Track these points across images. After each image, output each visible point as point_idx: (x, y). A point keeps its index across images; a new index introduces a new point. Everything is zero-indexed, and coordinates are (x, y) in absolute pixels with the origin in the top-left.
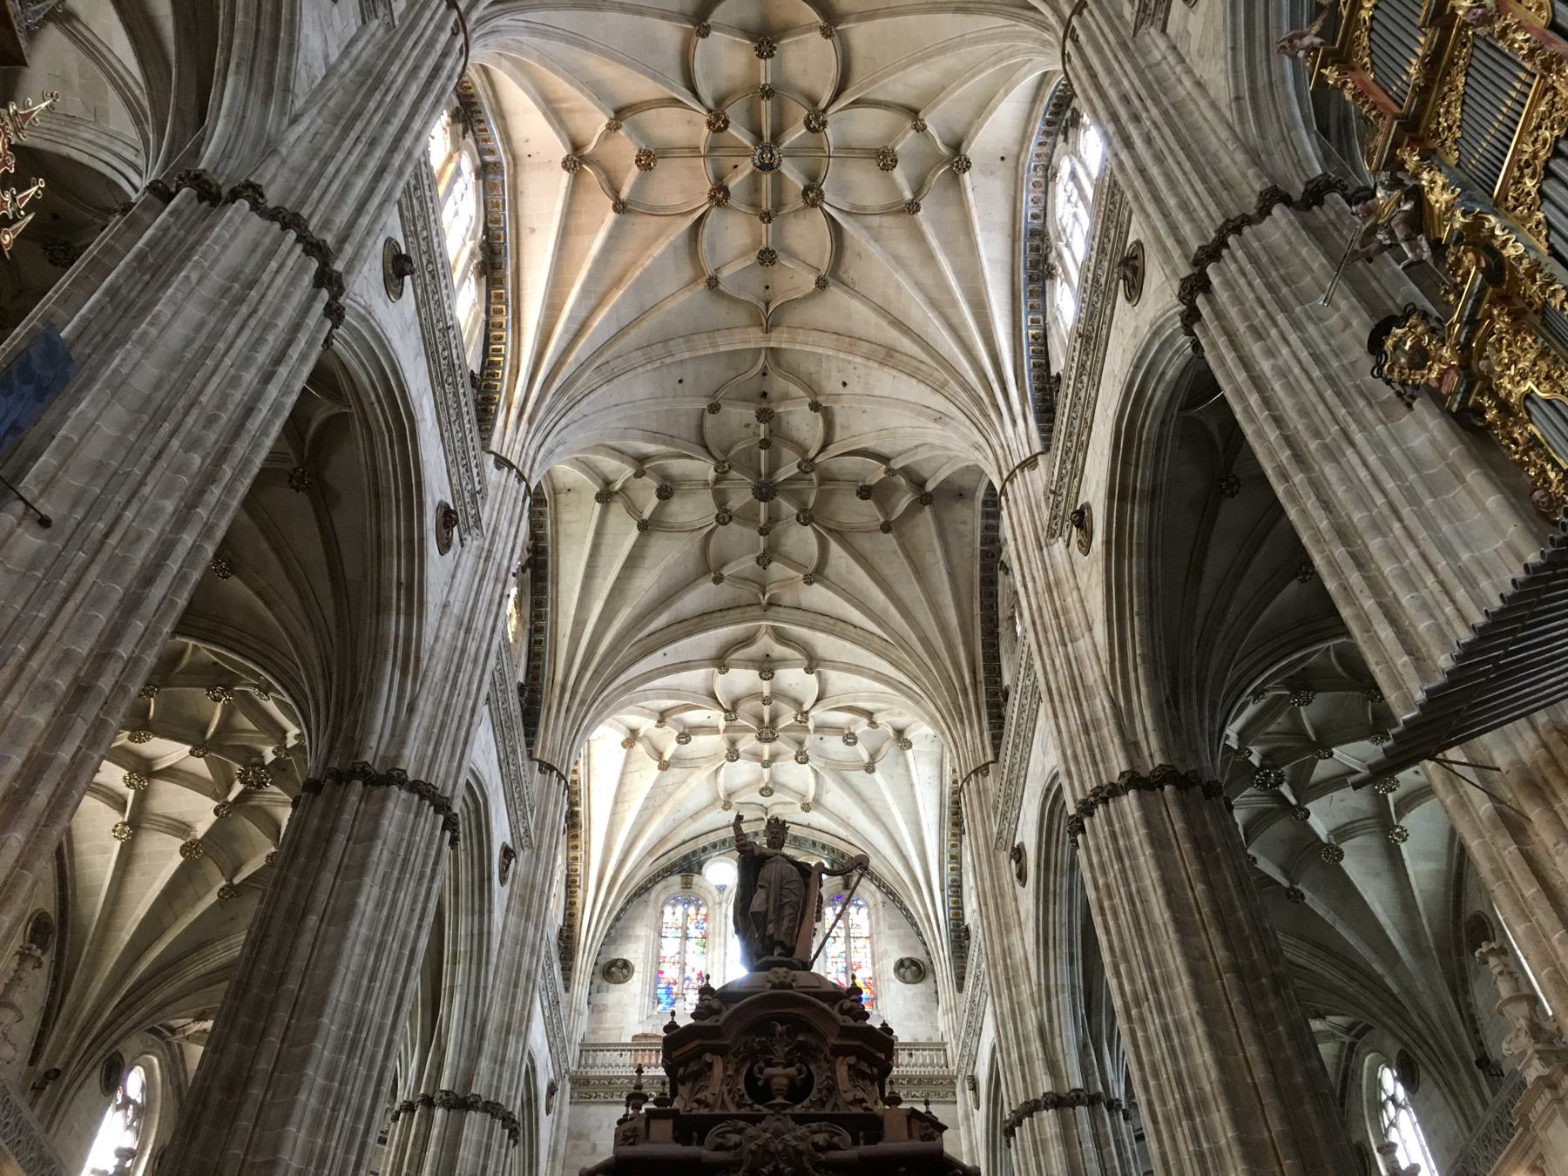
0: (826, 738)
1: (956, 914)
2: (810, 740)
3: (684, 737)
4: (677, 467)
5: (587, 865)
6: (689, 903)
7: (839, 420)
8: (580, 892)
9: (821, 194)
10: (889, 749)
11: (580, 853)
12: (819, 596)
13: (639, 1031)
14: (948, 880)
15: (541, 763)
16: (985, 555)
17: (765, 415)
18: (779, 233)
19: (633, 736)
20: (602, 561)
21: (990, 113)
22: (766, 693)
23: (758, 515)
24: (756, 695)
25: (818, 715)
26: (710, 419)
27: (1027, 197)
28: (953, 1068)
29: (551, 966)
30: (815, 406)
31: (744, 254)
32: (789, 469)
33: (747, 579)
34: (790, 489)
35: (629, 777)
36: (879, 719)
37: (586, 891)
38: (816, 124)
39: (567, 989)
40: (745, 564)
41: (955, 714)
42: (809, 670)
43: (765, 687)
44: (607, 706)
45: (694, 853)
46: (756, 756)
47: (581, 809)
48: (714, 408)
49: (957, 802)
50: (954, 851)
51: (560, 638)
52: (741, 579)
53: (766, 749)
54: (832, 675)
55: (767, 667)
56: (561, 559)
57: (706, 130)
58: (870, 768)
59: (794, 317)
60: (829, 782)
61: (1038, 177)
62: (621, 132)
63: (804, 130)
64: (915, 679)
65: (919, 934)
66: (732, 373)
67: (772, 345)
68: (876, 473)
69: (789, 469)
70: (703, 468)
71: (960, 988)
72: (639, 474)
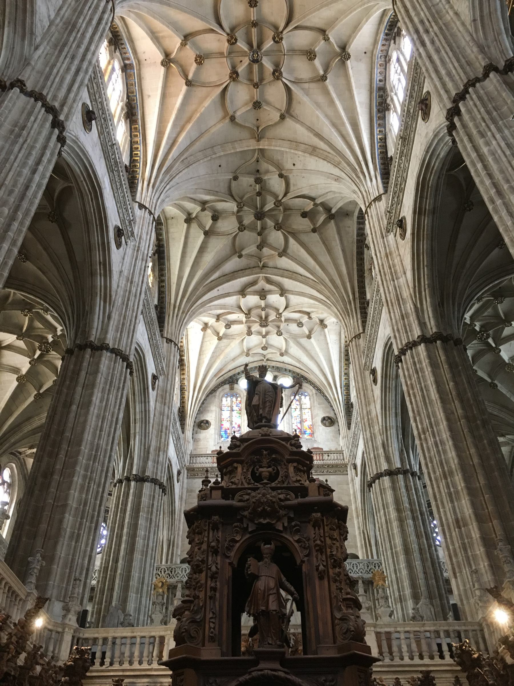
0: (290, 324)
1: (347, 398)
2: (283, 326)
3: (228, 326)
4: (220, 206)
7: (292, 182)
8: (186, 393)
9: (281, 74)
10: (317, 328)
11: (186, 376)
12: (285, 262)
14: (343, 384)
15: (167, 339)
16: (358, 241)
17: (258, 181)
18: (262, 94)
19: (206, 327)
20: (189, 250)
21: (359, 31)
22: (263, 306)
23: (257, 227)
24: (258, 307)
25: (286, 315)
26: (234, 183)
27: (377, 71)
28: (346, 461)
29: (176, 424)
30: (281, 176)
31: (246, 104)
32: (270, 205)
33: (253, 256)
34: (270, 214)
35: (205, 344)
36: (313, 315)
37: (189, 392)
38: (278, 39)
39: (183, 433)
40: (252, 249)
41: (346, 313)
42: (281, 295)
43: (263, 303)
44: (194, 313)
45: (234, 375)
46: (259, 333)
47: (185, 358)
48: (236, 178)
49: (347, 351)
50: (346, 371)
51: (172, 284)
52: (250, 256)
53: (264, 330)
54: (291, 297)
55: (263, 294)
56: (171, 249)
57: (227, 44)
58: (309, 337)
59: (270, 133)
60: (291, 343)
61: (382, 61)
62: (187, 47)
63: (272, 42)
65: (332, 406)
66: (243, 161)
67: (261, 147)
68: (309, 206)
69: (270, 205)
70: (231, 206)
71: (349, 428)
72: (203, 210)
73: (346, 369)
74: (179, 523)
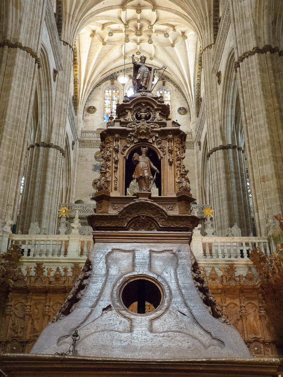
1: (198, 94)
2: (154, 35)
5: (80, 77)
6: (113, 89)
8: (78, 85)
10: (180, 39)
11: (78, 72)
13: (99, 128)
14: (196, 83)
15: (64, 42)
19: (94, 33)
22: (139, 18)
24: (134, 19)
25: (156, 27)
29: (71, 108)
36: (176, 28)
37: (80, 85)
42: (153, 10)
43: (139, 16)
44: (85, 22)
45: (115, 73)
46: (135, 41)
47: (77, 58)
49: (201, 58)
53: (139, 38)
55: (139, 8)
58: (173, 46)
60: (159, 49)
64: (189, 14)
65: (186, 100)
71: (198, 116)
73: (199, 72)
74: (74, 178)
